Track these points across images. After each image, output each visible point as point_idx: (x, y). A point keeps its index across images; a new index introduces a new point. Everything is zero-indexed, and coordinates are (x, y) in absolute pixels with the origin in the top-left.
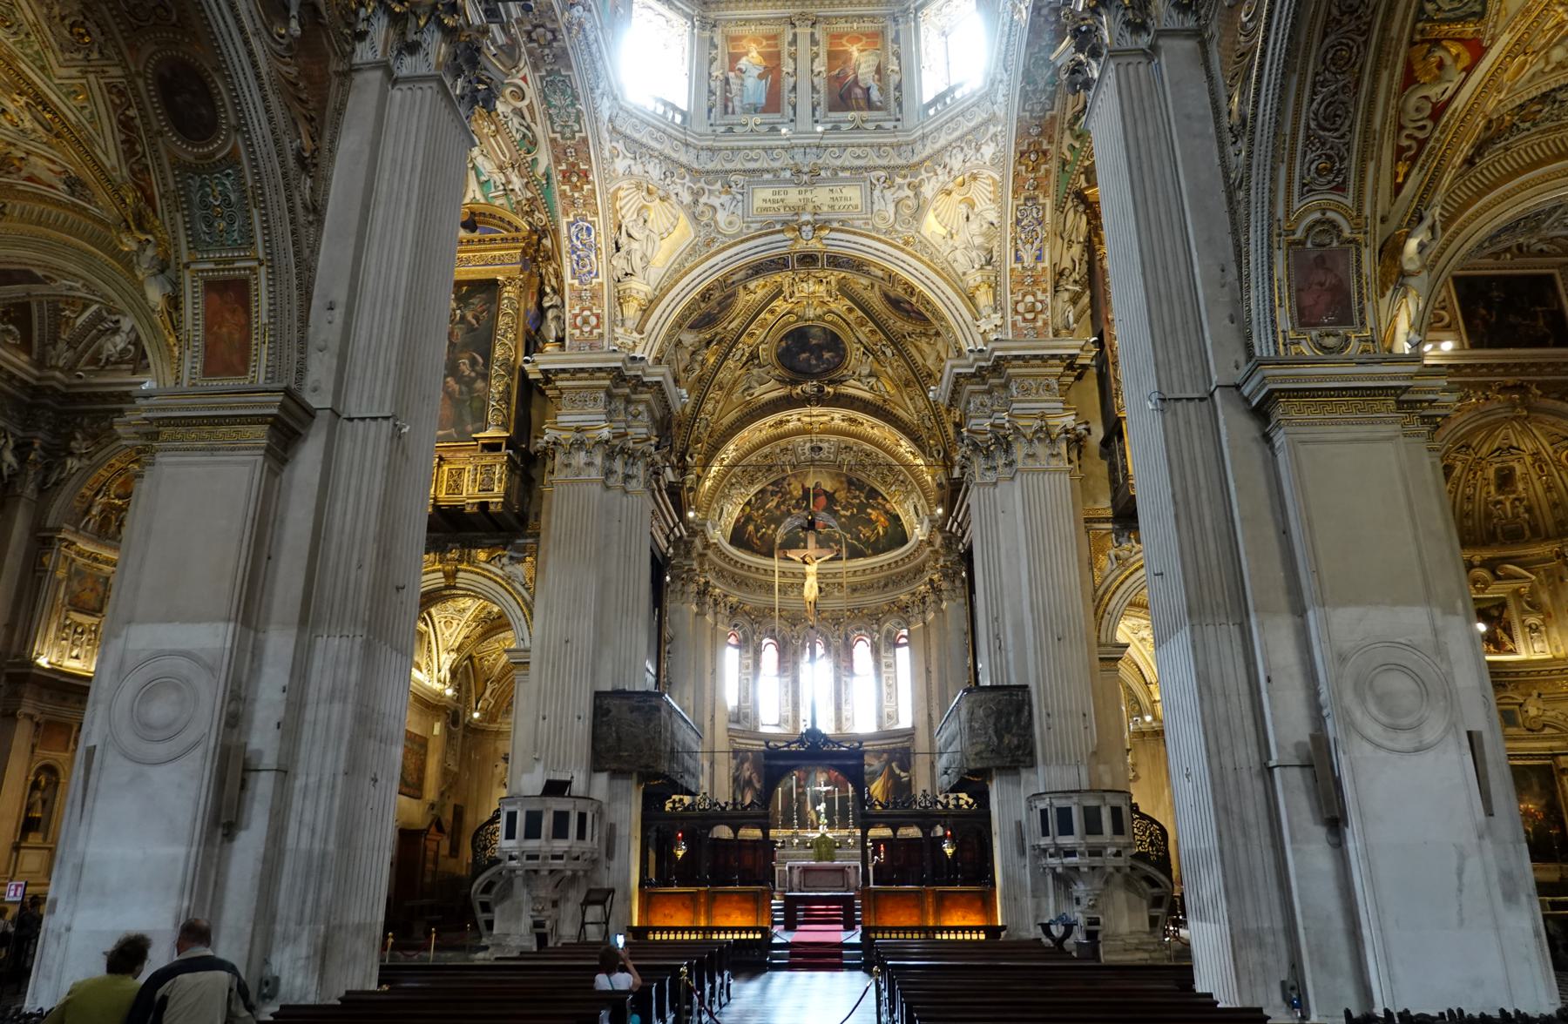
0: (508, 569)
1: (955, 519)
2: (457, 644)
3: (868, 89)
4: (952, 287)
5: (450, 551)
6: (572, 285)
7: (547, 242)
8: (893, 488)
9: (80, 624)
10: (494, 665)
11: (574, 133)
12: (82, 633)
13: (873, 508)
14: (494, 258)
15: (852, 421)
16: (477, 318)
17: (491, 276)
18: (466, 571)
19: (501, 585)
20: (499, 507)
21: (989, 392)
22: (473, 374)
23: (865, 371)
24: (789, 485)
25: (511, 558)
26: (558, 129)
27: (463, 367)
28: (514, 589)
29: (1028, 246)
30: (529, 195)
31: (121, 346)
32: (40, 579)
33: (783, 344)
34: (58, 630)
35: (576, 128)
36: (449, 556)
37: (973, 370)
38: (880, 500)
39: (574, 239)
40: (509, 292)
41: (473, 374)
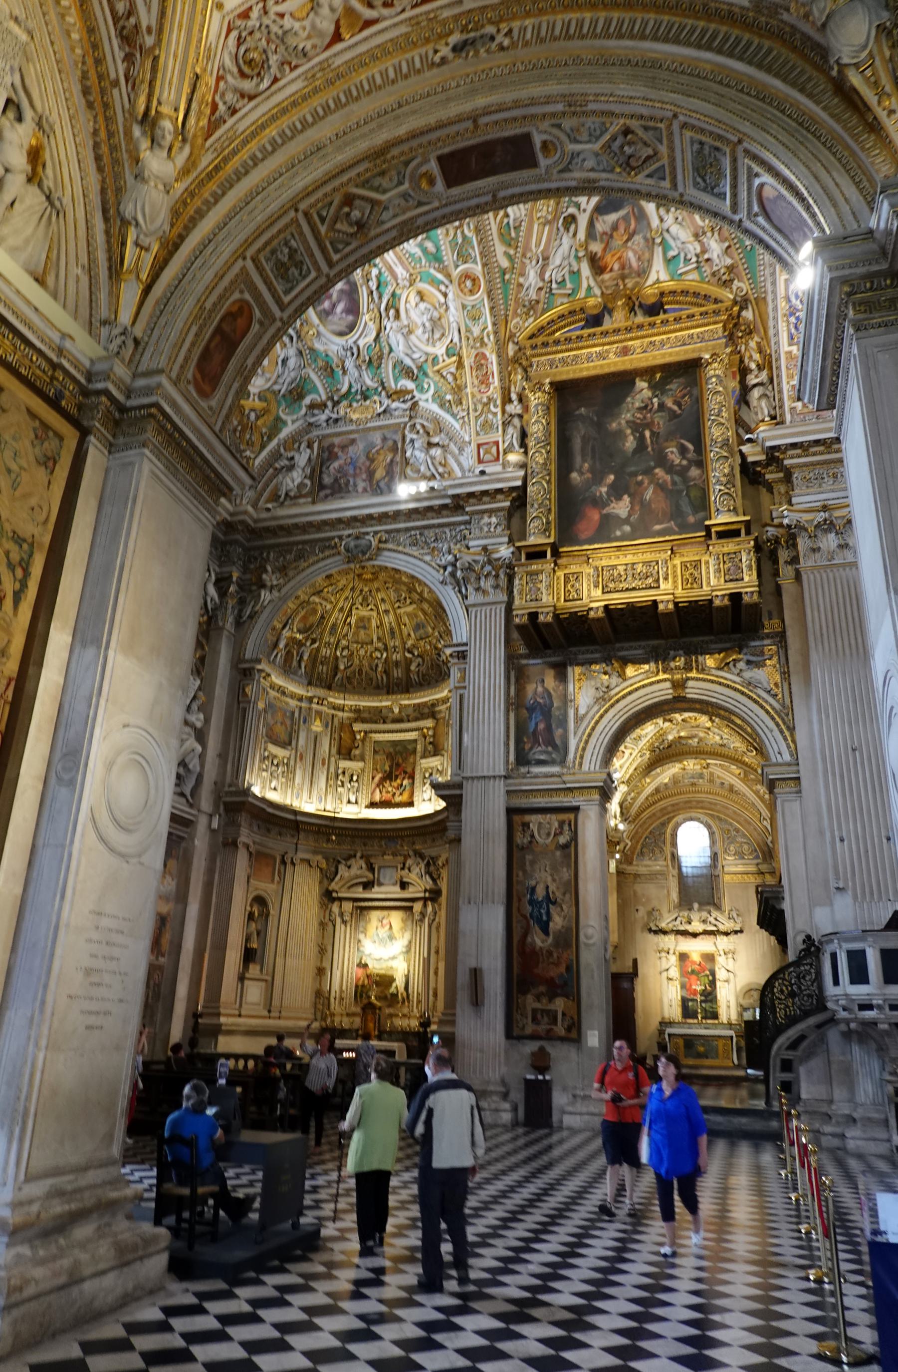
0: (748, 675)
2: (628, 776)
5: (674, 659)
6: (790, 352)
7: (748, 314)
9: (275, 757)
10: (631, 804)
12: (277, 765)
14: (691, 336)
16: (679, 405)
17: (695, 355)
18: (697, 679)
19: (743, 693)
20: (755, 597)
22: (685, 462)
25: (749, 662)
27: (671, 456)
28: (759, 696)
30: (729, 261)
31: (298, 481)
32: (245, 710)
34: (260, 761)
36: (672, 664)
40: (714, 370)
41: (685, 462)
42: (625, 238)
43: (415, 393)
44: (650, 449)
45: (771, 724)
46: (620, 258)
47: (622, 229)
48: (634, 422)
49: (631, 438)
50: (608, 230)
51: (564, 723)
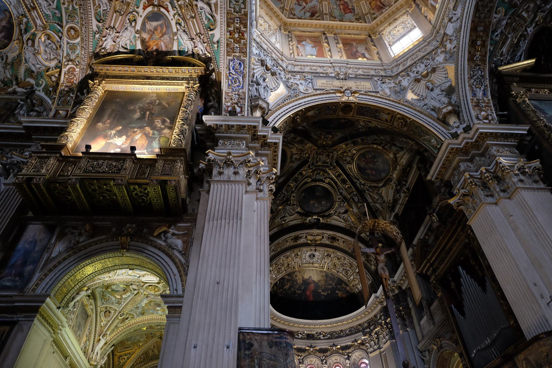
1: (429, 261)
3: (364, 54)
4: (431, 118)
8: (352, 277)
11: (240, 9)
13: (339, 290)
15: (333, 239)
21: (471, 160)
22: (163, 126)
23: (343, 211)
24: (296, 276)
26: (233, 6)
29: (478, 89)
33: (303, 194)
35: (243, 6)
37: (461, 147)
38: (344, 286)
39: (231, 69)
42: (160, 35)
43: (35, 87)
44: (146, 119)
45: (176, 271)
46: (157, 44)
47: (159, 31)
48: (143, 108)
49: (139, 113)
50: (152, 29)
51: (36, 262)
